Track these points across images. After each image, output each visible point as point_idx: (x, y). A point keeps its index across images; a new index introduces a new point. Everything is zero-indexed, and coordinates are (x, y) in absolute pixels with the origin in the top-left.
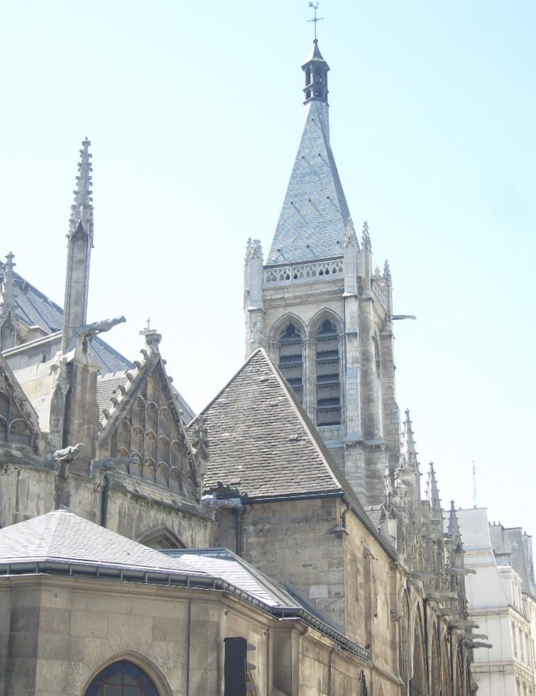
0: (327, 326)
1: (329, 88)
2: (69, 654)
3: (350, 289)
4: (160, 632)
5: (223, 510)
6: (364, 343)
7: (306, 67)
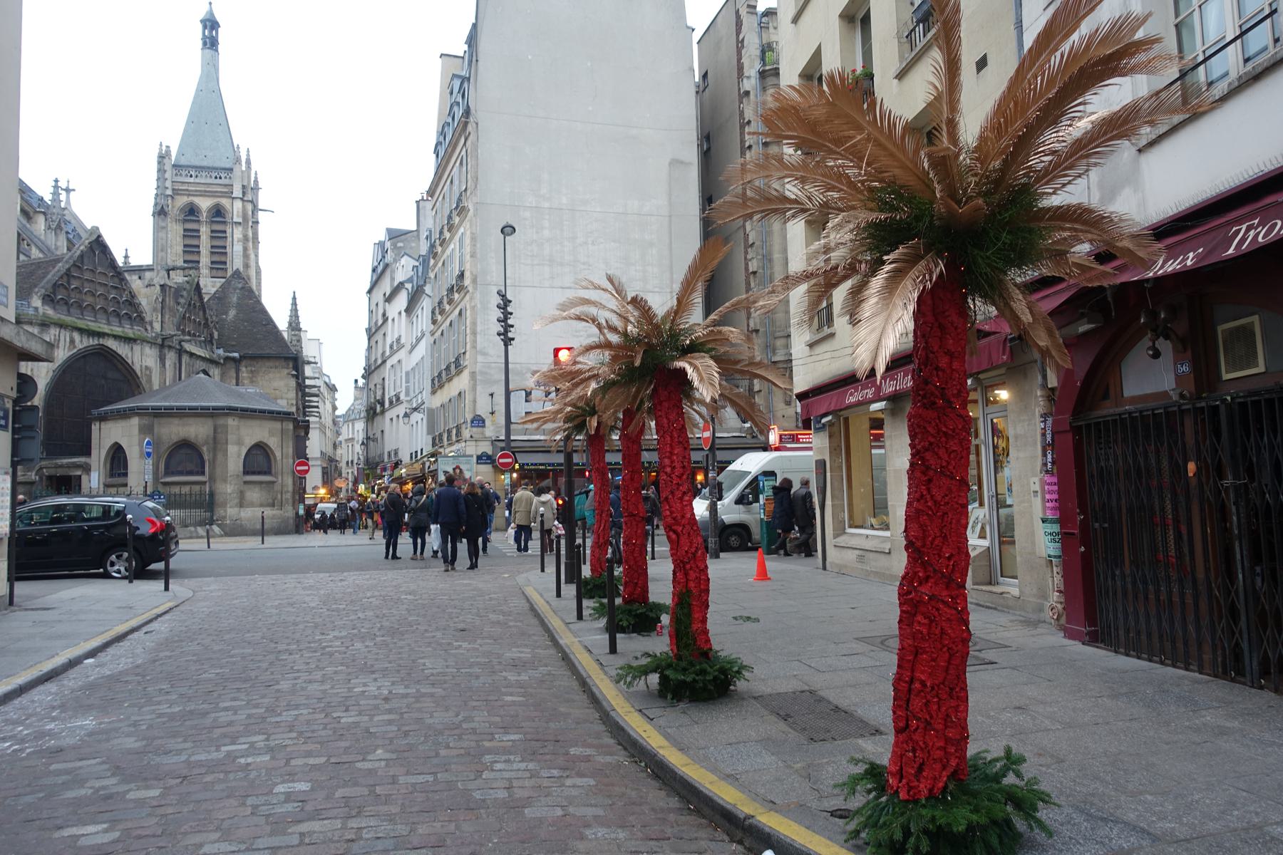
0: (218, 212)
1: (220, 40)
2: (239, 443)
3: (237, 192)
4: (271, 433)
5: (227, 359)
6: (245, 229)
7: (204, 22)
